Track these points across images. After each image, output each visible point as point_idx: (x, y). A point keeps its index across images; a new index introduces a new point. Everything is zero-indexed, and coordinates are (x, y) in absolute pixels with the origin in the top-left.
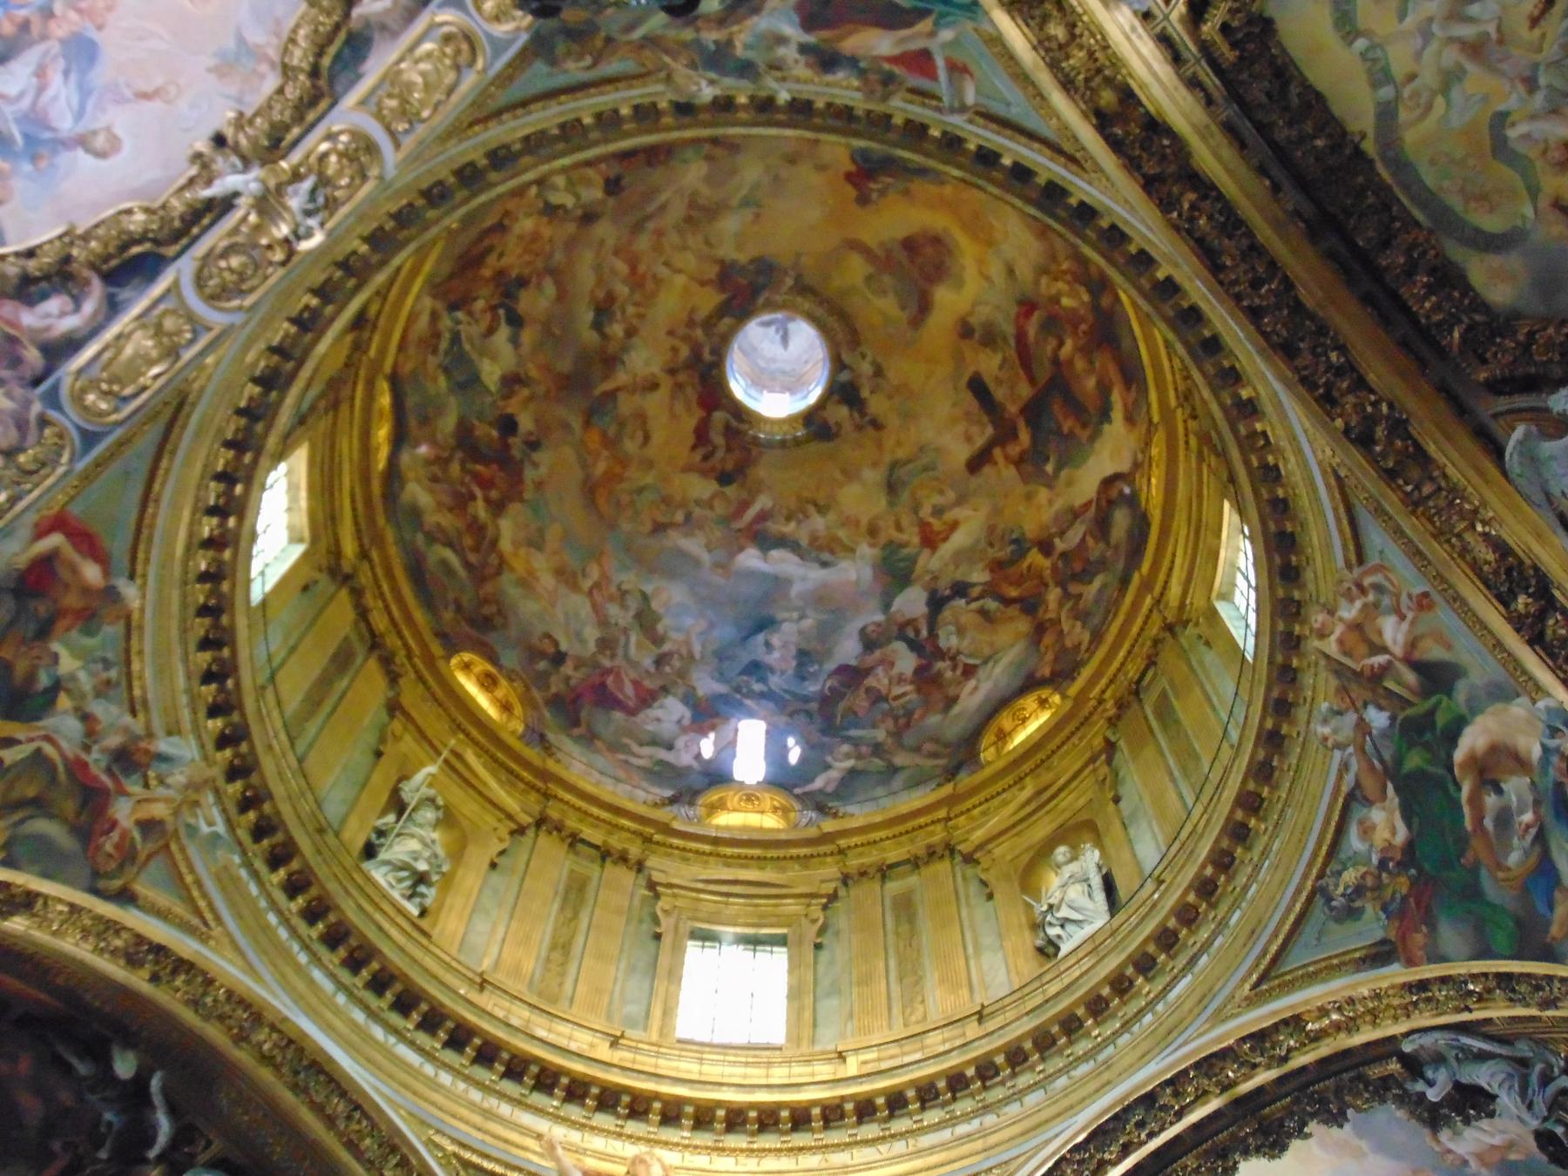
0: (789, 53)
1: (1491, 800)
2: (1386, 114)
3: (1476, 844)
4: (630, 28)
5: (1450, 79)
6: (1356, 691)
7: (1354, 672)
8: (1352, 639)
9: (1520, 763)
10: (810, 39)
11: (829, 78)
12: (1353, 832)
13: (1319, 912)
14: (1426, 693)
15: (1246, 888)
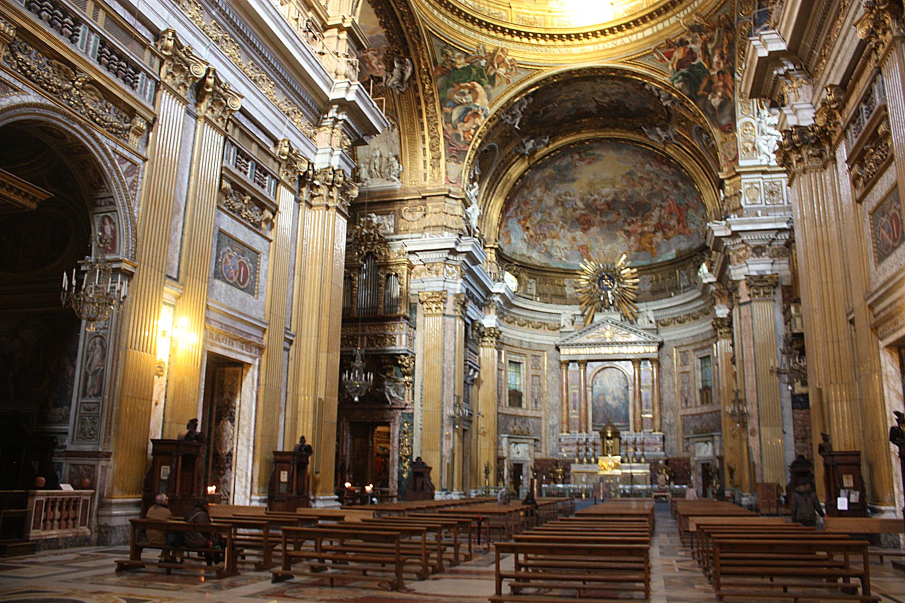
0: (689, 40)
1: (467, 91)
2: (595, 82)
3: (458, 87)
4: (719, 31)
5: (593, 88)
6: (489, 58)
7: (493, 59)
8: (501, 59)
9: (475, 100)
10: (689, 46)
11: (678, 38)
12: (459, 54)
13: (442, 45)
14: (488, 76)
15: (441, 13)
